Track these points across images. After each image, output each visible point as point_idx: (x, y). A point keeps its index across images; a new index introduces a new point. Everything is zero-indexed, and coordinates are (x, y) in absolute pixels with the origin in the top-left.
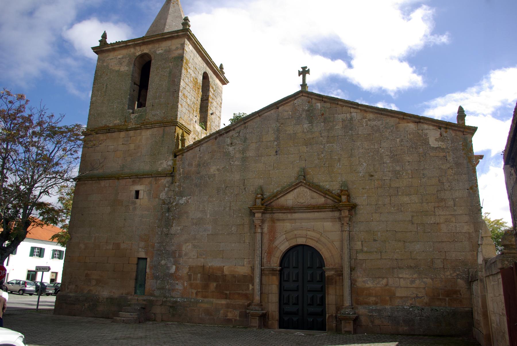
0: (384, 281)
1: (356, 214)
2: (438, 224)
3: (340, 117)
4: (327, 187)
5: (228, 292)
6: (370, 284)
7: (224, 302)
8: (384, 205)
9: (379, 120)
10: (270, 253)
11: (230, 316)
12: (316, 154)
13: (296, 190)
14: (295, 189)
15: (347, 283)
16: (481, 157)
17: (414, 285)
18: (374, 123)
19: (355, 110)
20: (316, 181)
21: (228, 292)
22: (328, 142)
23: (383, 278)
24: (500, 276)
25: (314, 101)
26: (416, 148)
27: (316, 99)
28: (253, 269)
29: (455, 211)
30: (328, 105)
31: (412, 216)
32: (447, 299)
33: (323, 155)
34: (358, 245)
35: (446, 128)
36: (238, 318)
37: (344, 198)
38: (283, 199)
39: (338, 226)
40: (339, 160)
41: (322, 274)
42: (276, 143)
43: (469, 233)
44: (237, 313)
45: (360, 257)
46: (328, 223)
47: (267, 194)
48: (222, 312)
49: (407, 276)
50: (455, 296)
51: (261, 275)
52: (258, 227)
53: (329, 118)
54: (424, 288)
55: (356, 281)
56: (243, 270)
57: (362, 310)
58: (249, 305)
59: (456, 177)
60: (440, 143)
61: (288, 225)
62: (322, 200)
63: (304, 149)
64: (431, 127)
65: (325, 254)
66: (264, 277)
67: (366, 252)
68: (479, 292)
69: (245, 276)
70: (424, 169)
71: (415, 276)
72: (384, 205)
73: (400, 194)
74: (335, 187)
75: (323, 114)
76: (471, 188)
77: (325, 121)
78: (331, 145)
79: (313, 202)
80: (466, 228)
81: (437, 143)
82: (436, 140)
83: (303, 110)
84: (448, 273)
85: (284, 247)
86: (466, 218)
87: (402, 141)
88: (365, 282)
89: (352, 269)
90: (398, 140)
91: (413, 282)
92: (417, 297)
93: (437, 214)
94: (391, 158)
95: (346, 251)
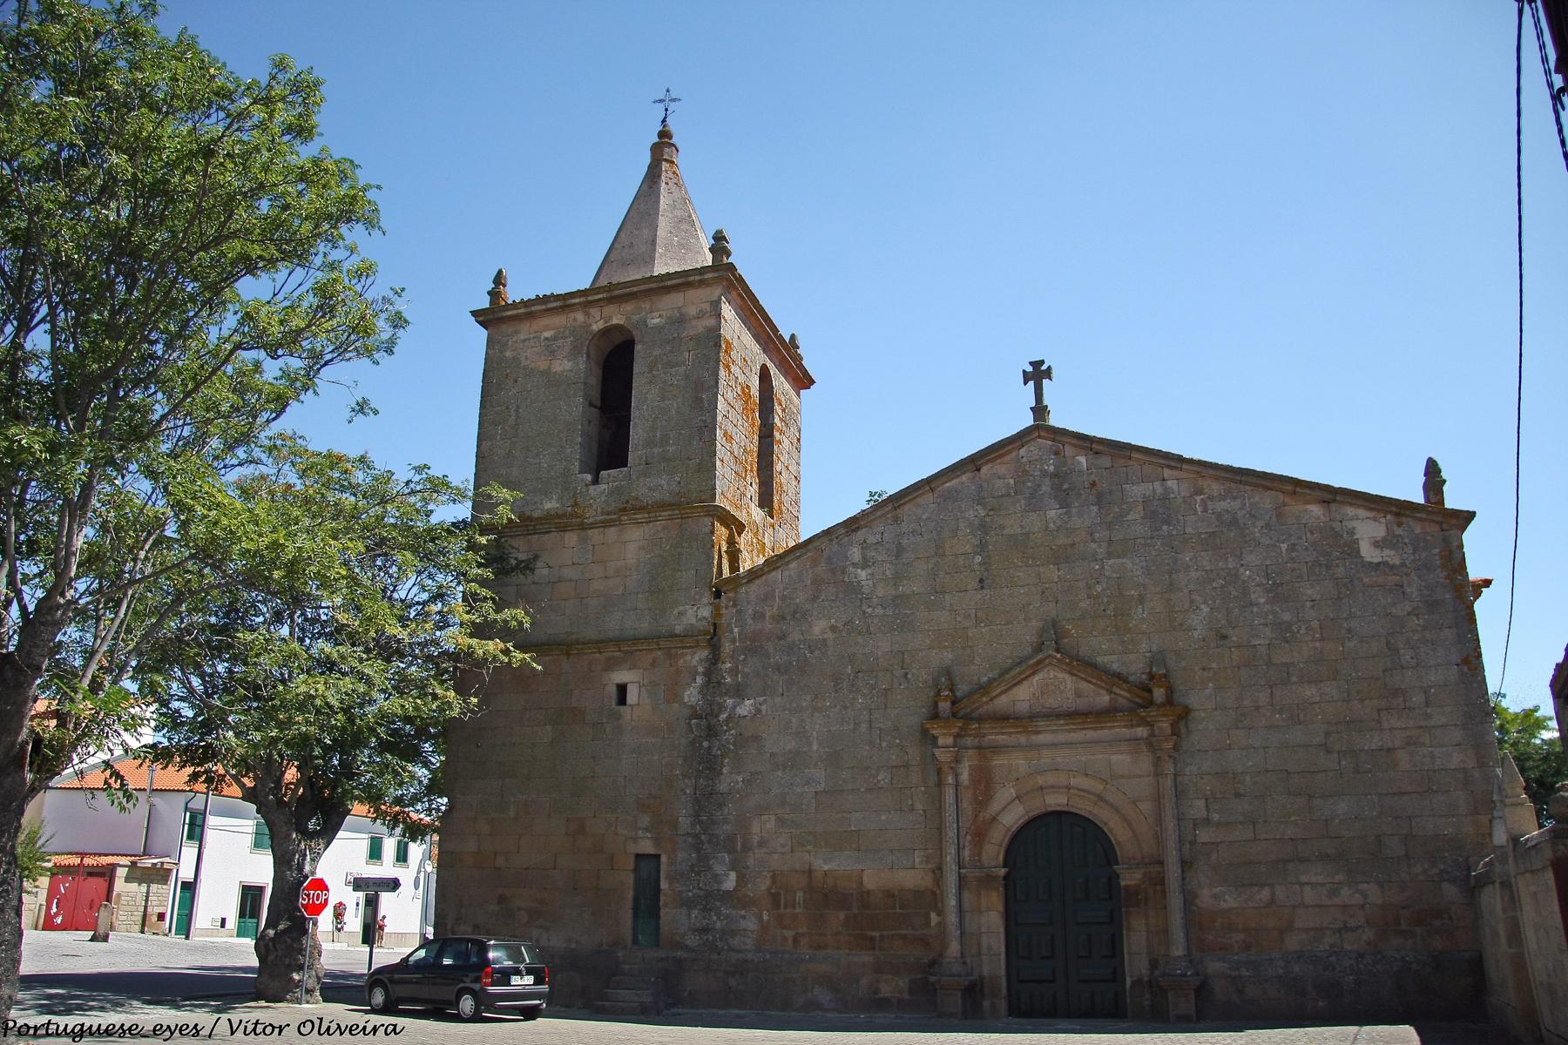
0: (1265, 894)
1: (1189, 732)
2: (1389, 750)
3: (1136, 491)
4: (1115, 666)
5: (876, 934)
6: (1230, 901)
7: (867, 958)
8: (1258, 708)
9: (1235, 498)
10: (980, 836)
11: (886, 990)
12: (1082, 584)
13: (1036, 678)
14: (1033, 674)
15: (1175, 901)
16: (1487, 583)
17: (1336, 901)
18: (1224, 505)
19: (1175, 473)
20: (1084, 651)
21: (876, 934)
22: (1110, 555)
23: (1262, 886)
24: (1549, 876)
25: (1069, 451)
26: (1327, 567)
27: (1075, 446)
28: (938, 872)
29: (1428, 717)
30: (1106, 461)
31: (1327, 734)
32: (1418, 930)
33: (1099, 588)
34: (1197, 808)
35: (1397, 515)
36: (906, 996)
37: (1159, 694)
38: (1003, 699)
39: (1145, 763)
40: (1141, 600)
41: (1113, 879)
42: (978, 559)
43: (1465, 771)
44: (903, 983)
45: (1204, 835)
46: (1121, 757)
47: (963, 689)
48: (864, 982)
49: (1321, 879)
50: (1437, 923)
51: (960, 888)
52: (945, 768)
53: (1111, 493)
54: (1363, 906)
55: (1196, 896)
56: (912, 877)
57: (1214, 966)
58: (933, 963)
59: (1428, 635)
60: (1387, 552)
61: (1021, 763)
62: (1104, 699)
63: (1053, 573)
64: (1362, 513)
65: (1118, 832)
66: (966, 895)
67: (1219, 824)
68: (1499, 912)
69: (918, 893)
70: (1351, 617)
71: (1339, 878)
72: (1258, 708)
73: (1294, 679)
74: (1135, 666)
75: (1093, 484)
76: (1466, 661)
77: (1100, 500)
78: (1118, 561)
79: (1082, 704)
80: (1456, 760)
81: (1378, 552)
82: (1377, 544)
83: (1044, 473)
84: (1418, 869)
85: (1013, 818)
86: (1457, 735)
87: (1292, 548)
88: (1215, 896)
89: (1186, 864)
90: (1284, 547)
91: (1333, 893)
92: (1346, 928)
93: (1385, 725)
94: (1269, 591)
95: (1170, 824)
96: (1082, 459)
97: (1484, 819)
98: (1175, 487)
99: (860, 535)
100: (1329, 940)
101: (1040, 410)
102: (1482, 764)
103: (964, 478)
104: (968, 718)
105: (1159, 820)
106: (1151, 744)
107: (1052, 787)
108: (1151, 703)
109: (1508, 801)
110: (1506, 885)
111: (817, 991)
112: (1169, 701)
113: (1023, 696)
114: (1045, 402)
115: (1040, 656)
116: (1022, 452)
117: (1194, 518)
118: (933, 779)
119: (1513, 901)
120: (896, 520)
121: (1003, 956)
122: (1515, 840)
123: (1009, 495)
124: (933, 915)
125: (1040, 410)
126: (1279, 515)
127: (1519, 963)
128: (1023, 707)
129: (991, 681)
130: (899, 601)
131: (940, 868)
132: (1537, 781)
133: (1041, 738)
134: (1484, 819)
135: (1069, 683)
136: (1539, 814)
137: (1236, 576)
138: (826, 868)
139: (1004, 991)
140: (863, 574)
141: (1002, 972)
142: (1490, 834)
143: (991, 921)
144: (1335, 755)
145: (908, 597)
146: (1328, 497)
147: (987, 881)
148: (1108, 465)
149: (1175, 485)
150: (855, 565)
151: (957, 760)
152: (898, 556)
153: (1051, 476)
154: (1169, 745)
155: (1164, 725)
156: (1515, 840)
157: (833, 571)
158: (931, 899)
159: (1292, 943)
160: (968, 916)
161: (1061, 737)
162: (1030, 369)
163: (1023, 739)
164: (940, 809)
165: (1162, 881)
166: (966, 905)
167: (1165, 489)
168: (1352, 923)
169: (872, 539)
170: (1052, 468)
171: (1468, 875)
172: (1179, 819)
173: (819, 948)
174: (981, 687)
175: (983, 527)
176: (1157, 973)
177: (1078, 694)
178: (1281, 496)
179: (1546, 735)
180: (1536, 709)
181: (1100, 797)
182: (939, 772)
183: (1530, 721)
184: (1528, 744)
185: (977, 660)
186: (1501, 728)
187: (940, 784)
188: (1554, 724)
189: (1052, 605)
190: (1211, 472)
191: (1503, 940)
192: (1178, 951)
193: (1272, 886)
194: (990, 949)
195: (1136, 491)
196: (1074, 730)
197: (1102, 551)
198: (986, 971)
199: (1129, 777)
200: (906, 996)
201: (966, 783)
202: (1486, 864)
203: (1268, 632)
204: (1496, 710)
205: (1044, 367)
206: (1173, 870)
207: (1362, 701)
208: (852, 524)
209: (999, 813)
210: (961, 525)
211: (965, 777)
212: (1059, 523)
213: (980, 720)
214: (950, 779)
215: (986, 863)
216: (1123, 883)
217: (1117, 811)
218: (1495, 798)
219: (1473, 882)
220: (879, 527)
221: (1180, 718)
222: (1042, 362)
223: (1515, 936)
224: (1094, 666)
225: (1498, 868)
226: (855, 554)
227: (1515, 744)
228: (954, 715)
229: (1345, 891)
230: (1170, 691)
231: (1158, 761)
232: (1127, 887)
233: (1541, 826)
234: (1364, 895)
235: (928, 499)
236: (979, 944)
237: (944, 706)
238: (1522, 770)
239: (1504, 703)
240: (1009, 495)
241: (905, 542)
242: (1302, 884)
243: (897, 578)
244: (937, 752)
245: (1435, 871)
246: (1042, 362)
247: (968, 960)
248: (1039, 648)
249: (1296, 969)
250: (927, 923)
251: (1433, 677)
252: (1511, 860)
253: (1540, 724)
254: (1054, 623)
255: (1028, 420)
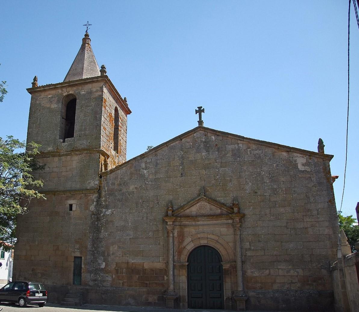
0: (267, 272)
1: (245, 222)
2: (306, 228)
3: (230, 147)
4: (222, 201)
5: (148, 282)
6: (256, 274)
7: (145, 289)
8: (266, 215)
9: (260, 150)
10: (180, 252)
11: (150, 300)
12: (213, 176)
13: (198, 204)
14: (197, 203)
15: (240, 273)
16: (337, 177)
17: (289, 274)
18: (257, 152)
19: (242, 142)
20: (213, 196)
21: (148, 282)
22: (221, 167)
23: (266, 269)
24: (355, 267)
25: (209, 135)
26: (288, 172)
27: (211, 133)
28: (167, 263)
29: (318, 218)
30: (220, 138)
31: (287, 223)
32: (314, 284)
33: (218, 177)
34: (247, 245)
35: (310, 156)
36: (157, 301)
37: (236, 210)
38: (188, 210)
39: (231, 231)
40: (231, 181)
41: (221, 266)
42: (181, 167)
43: (329, 235)
44: (156, 297)
45: (249, 253)
46: (224, 229)
47: (175, 207)
48: (144, 297)
49: (284, 267)
50: (320, 281)
51: (174, 269)
52: (170, 232)
53: (222, 148)
54: (297, 276)
55: (246, 272)
56: (159, 265)
57: (251, 294)
58: (165, 291)
59: (319, 193)
60: (306, 167)
61: (193, 230)
62: (219, 211)
63: (204, 172)
64: (299, 155)
65: (222, 252)
66: (175, 271)
67: (253, 250)
68: (339, 278)
69: (161, 270)
70: (295, 187)
71: (290, 267)
72: (266, 215)
73: (277, 206)
74: (228, 201)
75: (217, 145)
76: (330, 201)
77: (218, 150)
78: (224, 169)
79: (212, 212)
80: (327, 231)
81: (304, 167)
82: (303, 165)
83: (202, 141)
84: (314, 265)
85: (190, 247)
86: (327, 224)
87: (277, 166)
88: (252, 272)
89: (243, 262)
90: (275, 165)
91: (288, 272)
92: (292, 283)
93: (305, 220)
94: (270, 179)
95: (238, 250)
96: (213, 137)
97: (335, 250)
98: (242, 146)
99: (145, 159)
100: (286, 286)
101: (200, 122)
102: (334, 233)
103: (177, 142)
104: (177, 216)
105: (235, 249)
106: (233, 225)
107: (202, 238)
108: (233, 212)
109: (342, 244)
110: (341, 270)
111: (129, 299)
112: (239, 212)
113: (194, 210)
114: (202, 120)
115: (199, 198)
116: (195, 135)
117: (247, 156)
118: (166, 235)
119: (343, 275)
120: (156, 155)
121: (187, 290)
122: (344, 256)
123: (191, 148)
124: (165, 277)
125: (200, 122)
126: (273, 155)
127: (345, 294)
128: (194, 213)
129: (184, 205)
130: (156, 180)
131: (168, 262)
132: (351, 238)
133: (199, 223)
134: (335, 250)
135: (208, 206)
136: (352, 249)
137: (260, 174)
138: (133, 262)
139: (187, 300)
140: (145, 171)
141: (186, 295)
142: (337, 255)
143: (183, 279)
144: (290, 229)
145: (159, 179)
146: (289, 150)
147: (182, 266)
148: (221, 139)
149: (242, 146)
150: (143, 169)
151: (173, 229)
152: (156, 166)
153: (203, 142)
154: (239, 225)
155: (237, 219)
156: (344, 256)
157: (136, 170)
158: (165, 272)
159: (275, 287)
160: (176, 277)
161: (205, 223)
162: (198, 109)
163: (194, 223)
164: (168, 244)
165: (236, 267)
166: (176, 274)
167: (239, 147)
168: (294, 281)
169: (148, 161)
170: (204, 140)
171: (330, 267)
172: (241, 248)
173: (130, 286)
174: (181, 207)
175: (183, 158)
176: (234, 295)
177: (211, 209)
178: (274, 149)
179: (354, 224)
180: (351, 216)
181: (217, 241)
182: (168, 233)
183: (349, 220)
184: (349, 227)
185: (180, 199)
186: (341, 222)
187: (168, 236)
188: (357, 221)
189: (203, 182)
190: (253, 142)
191: (340, 287)
192: (240, 289)
193: (269, 269)
194: (183, 287)
195: (230, 147)
196: (209, 221)
197: (219, 166)
198: (181, 294)
199: (226, 235)
200: (157, 301)
201: (176, 236)
202: (335, 264)
203: (269, 191)
204: (339, 216)
205: (202, 109)
206: (239, 264)
207: (298, 213)
208: (142, 156)
209: (186, 246)
210: (176, 157)
211: (176, 234)
212: (206, 157)
213: (181, 217)
214: (171, 235)
215: (182, 261)
216: (224, 268)
217: (222, 245)
218: (338, 243)
219: (331, 269)
220: (150, 157)
221: (242, 217)
222: (201, 107)
223: (344, 286)
224: (216, 201)
225: (339, 265)
226: (143, 165)
227: (345, 227)
228: (173, 215)
229: (292, 271)
230: (239, 209)
231: (235, 231)
232: (225, 269)
233: (352, 252)
234: (298, 272)
235: (166, 149)
236: (179, 286)
237: (170, 212)
238: (347, 235)
239: (342, 214)
240: (191, 148)
241: (158, 162)
242: (279, 269)
243: (156, 173)
244: (167, 226)
245: (320, 265)
246: (201, 107)
247: (176, 291)
248: (199, 195)
249: (277, 295)
250: (164, 279)
251: (320, 206)
252: (343, 263)
253: (352, 221)
254: (204, 187)
255: (197, 125)
